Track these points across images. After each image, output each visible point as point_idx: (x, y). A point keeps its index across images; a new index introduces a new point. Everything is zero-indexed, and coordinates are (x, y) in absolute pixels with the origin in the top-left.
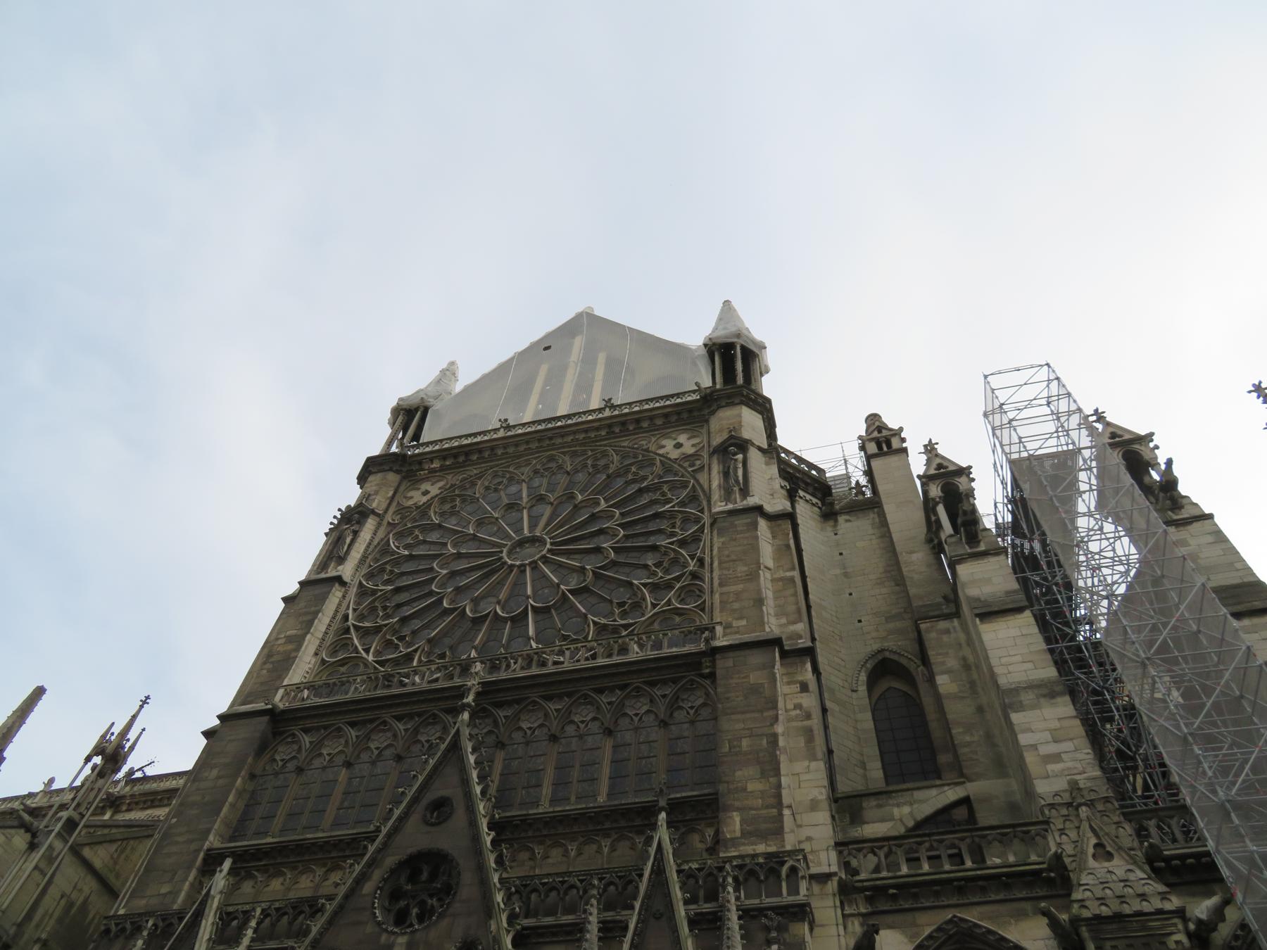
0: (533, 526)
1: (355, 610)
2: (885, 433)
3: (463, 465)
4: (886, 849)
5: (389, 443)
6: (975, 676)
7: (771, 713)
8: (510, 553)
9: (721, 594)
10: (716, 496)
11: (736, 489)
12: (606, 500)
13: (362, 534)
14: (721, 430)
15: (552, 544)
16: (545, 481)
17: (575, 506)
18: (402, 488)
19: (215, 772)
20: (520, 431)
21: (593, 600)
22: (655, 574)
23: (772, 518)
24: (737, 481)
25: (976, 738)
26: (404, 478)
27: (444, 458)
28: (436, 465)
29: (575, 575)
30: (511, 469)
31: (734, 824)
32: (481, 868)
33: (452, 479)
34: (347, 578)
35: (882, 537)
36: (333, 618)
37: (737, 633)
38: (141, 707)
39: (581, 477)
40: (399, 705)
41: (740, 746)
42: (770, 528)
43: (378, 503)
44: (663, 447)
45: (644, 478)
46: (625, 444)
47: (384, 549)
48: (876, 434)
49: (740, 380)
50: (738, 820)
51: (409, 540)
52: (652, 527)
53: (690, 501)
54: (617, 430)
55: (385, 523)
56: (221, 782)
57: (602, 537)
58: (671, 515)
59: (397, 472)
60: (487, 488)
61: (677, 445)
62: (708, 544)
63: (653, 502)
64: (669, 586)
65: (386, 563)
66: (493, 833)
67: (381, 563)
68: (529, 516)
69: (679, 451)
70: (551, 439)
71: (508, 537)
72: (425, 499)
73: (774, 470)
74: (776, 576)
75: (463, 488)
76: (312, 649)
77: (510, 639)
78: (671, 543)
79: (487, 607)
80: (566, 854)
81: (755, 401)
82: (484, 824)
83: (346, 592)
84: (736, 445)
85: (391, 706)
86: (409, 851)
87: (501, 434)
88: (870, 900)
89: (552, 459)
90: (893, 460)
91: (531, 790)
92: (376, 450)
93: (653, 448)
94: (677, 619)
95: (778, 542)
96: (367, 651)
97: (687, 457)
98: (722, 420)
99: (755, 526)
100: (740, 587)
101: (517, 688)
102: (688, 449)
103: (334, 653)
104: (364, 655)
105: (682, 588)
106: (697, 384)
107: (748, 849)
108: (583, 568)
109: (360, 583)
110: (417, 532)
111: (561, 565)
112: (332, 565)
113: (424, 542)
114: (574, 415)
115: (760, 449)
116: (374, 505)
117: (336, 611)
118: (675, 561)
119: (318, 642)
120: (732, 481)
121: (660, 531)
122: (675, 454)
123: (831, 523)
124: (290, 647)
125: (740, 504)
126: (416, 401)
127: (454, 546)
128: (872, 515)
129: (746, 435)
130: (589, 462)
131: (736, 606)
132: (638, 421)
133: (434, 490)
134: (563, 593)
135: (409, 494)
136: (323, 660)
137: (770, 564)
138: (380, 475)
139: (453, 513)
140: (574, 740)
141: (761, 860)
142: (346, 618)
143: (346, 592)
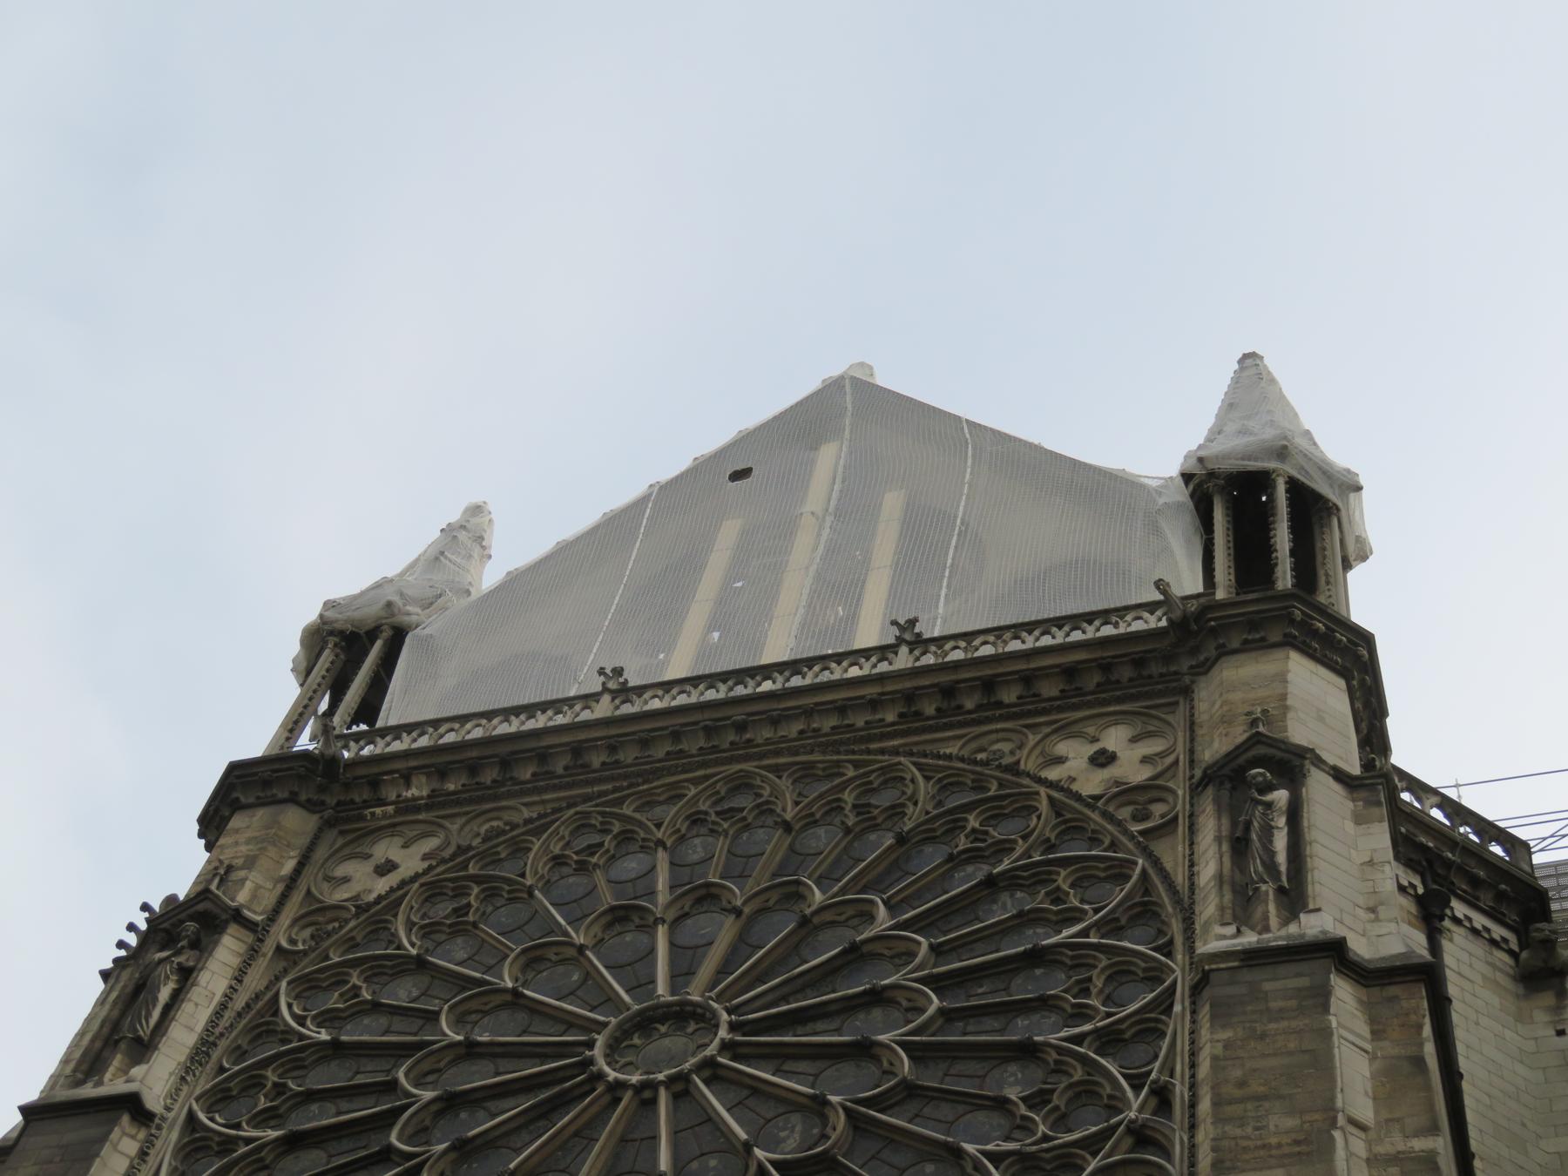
0: (680, 975)
5: (293, 726)
10: (1208, 907)
11: (1268, 888)
13: (204, 978)
14: (1226, 720)
15: (733, 1027)
16: (721, 845)
17: (804, 921)
18: (321, 853)
20: (656, 704)
22: (1026, 1126)
23: (1368, 976)
24: (1271, 867)
26: (328, 824)
27: (442, 773)
29: (796, 1119)
30: (627, 810)
33: (462, 831)
34: (154, 1101)
39: (823, 839)
42: (1367, 1007)
43: (251, 892)
44: (1060, 760)
45: (1004, 848)
47: (263, 1023)
49: (1285, 578)
51: (334, 1001)
52: (1023, 988)
53: (1134, 920)
54: (930, 709)
55: (268, 948)
57: (877, 1013)
58: (1076, 958)
59: (311, 806)
60: (558, 861)
61: (1097, 758)
62: (1183, 1044)
63: (1025, 919)
67: (251, 1058)
68: (672, 944)
70: (741, 727)
71: (610, 1001)
72: (382, 885)
73: (1380, 838)
74: (1380, 1149)
78: (1078, 1039)
81: (1327, 640)
84: (1266, 763)
87: (603, 709)
89: (742, 784)
92: (255, 743)
93: (1029, 765)
95: (1389, 1048)
97: (1126, 793)
98: (1233, 688)
99: (1321, 998)
102: (1132, 767)
106: (1160, 585)
108: (818, 1106)
109: (191, 1116)
110: (355, 979)
111: (757, 1089)
112: (117, 1061)
113: (376, 1007)
114: (810, 662)
115: (1339, 775)
116: (242, 897)
118: (1086, 1093)
120: (1256, 866)
121: (1044, 1003)
122: (1092, 783)
123: (1548, 998)
125: (1279, 934)
126: (372, 612)
127: (459, 1021)
129: (1299, 732)
130: (848, 797)
132: (989, 685)
133: (410, 861)
135: (340, 871)
137: (1365, 1111)
138: (261, 814)
139: (459, 927)
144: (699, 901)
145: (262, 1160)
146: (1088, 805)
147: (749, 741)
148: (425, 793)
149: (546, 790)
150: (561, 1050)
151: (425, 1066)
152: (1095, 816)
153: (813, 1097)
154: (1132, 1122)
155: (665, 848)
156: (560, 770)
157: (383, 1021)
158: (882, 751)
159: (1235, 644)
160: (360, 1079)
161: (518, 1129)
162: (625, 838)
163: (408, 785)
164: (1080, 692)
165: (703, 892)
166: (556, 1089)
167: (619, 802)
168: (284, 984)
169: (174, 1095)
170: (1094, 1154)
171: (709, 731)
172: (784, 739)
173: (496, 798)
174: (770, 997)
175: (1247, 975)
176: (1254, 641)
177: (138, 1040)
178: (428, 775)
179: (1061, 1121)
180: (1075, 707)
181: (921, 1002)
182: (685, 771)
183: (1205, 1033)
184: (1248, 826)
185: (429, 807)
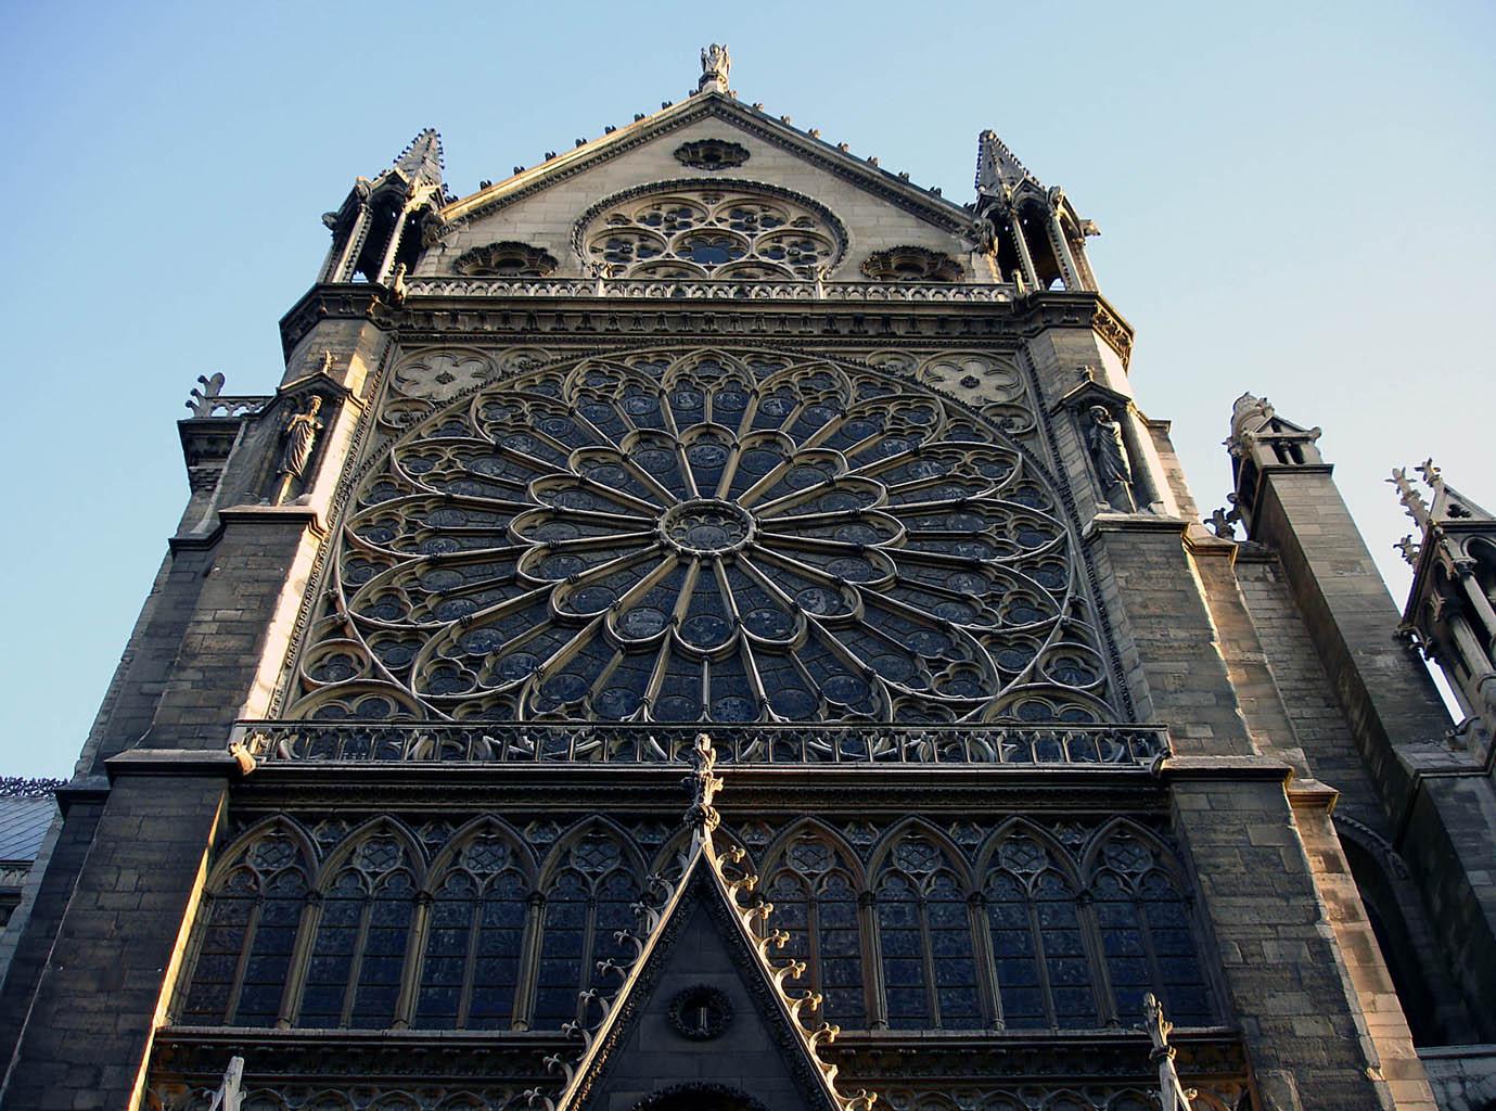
1: (349, 592)
2: (1286, 432)
5: (330, 270)
7: (1303, 901)
10: (1084, 490)
19: (129, 878)
24: (1123, 470)
27: (482, 318)
29: (818, 593)
40: (518, 795)
41: (1261, 954)
48: (1269, 432)
50: (1291, 1082)
56: (148, 899)
58: (993, 511)
62: (1084, 576)
65: (397, 505)
69: (973, 393)
70: (709, 320)
72: (446, 392)
78: (1011, 564)
85: (501, 795)
86: (660, 1085)
90: (1311, 485)
94: (1057, 709)
101: (775, 794)
104: (399, 684)
108: (838, 583)
122: (968, 397)
124: (232, 643)
131: (1184, 699)
134: (810, 623)
136: (301, 679)
138: (343, 324)
142: (331, 604)
145: (414, 573)
146: (972, 412)
147: (716, 331)
150: (628, 525)
154: (1063, 621)
155: (757, 397)
156: (572, 329)
158: (813, 353)
159: (1055, 322)
165: (705, 430)
166: (640, 551)
172: (740, 334)
174: (776, 509)
175: (1124, 537)
176: (1070, 322)
178: (470, 317)
180: (945, 345)
182: (668, 345)
183: (1104, 570)
184: (1099, 441)
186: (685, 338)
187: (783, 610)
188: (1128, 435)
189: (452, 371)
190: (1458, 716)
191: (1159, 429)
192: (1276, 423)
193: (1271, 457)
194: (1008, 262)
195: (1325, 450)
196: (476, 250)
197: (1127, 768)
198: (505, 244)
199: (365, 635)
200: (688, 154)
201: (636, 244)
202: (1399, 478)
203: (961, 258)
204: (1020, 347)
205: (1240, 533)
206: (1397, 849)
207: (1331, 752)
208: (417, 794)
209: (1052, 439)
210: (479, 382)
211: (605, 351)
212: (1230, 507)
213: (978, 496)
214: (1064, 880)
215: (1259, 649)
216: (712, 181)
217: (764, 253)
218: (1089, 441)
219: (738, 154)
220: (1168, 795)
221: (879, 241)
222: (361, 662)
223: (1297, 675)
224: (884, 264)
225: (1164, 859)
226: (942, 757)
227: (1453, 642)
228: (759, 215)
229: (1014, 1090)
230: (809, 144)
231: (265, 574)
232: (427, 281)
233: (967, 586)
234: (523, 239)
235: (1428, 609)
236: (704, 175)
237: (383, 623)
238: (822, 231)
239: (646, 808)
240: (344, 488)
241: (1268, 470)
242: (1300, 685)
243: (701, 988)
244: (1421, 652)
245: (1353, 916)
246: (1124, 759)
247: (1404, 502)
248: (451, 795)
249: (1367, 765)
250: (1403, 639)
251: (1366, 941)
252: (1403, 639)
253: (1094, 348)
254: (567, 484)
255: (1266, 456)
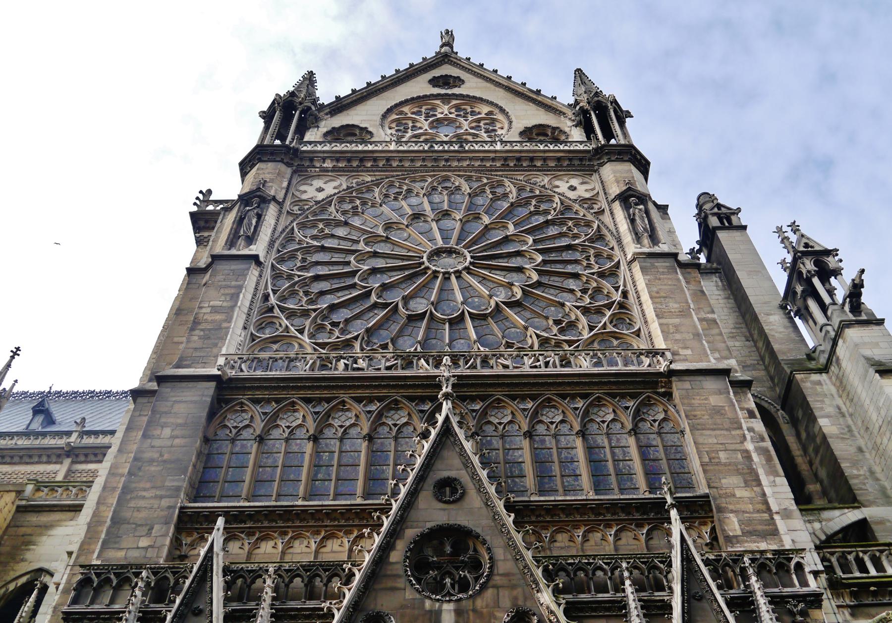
0: (445, 239)
1: (275, 292)
3: (357, 170)
4: (854, 554)
5: (263, 138)
6: (850, 422)
8: (429, 259)
9: (660, 325)
12: (516, 225)
15: (472, 257)
18: (294, 182)
21: (528, 314)
25: (862, 472)
26: (294, 172)
27: (338, 160)
28: (328, 164)
29: (501, 289)
30: (406, 182)
31: (733, 525)
32: (511, 545)
33: (343, 182)
34: (262, 259)
35: (728, 298)
36: (255, 295)
37: (686, 360)
38: (13, 357)
40: (359, 387)
46: (521, 178)
48: (716, 210)
50: (735, 520)
52: (566, 256)
53: (597, 239)
55: (284, 211)
59: (288, 165)
61: (570, 187)
62: (629, 279)
63: (562, 235)
64: (599, 311)
66: (513, 515)
70: (447, 160)
72: (320, 196)
75: (359, 191)
76: (241, 324)
77: (451, 341)
78: (593, 274)
79: (420, 306)
80: (571, 540)
82: (500, 505)
83: (261, 271)
85: (350, 388)
86: (429, 525)
88: (854, 595)
90: (736, 234)
91: (517, 480)
94: (615, 343)
96: (301, 332)
100: (677, 321)
102: (583, 191)
103: (260, 328)
104: (299, 336)
105: (613, 315)
107: (753, 546)
116: (272, 193)
117: (256, 289)
119: (244, 316)
121: (576, 262)
122: (572, 195)
128: (715, 279)
133: (330, 189)
134: (497, 303)
136: (252, 333)
139: (355, 212)
140: (547, 438)
141: (769, 556)
142: (266, 297)
143: (261, 271)
144: (444, 215)
148: (331, 166)
149: (377, 171)
150: (410, 258)
151: (359, 258)
152: (577, 205)
153: (508, 283)
156: (381, 165)
157: (336, 241)
159: (613, 159)
160: (333, 260)
161: (401, 283)
162: (409, 191)
163: (324, 162)
164: (561, 166)
167: (405, 179)
168: (295, 224)
169: (266, 257)
170: (609, 309)
171: (436, 160)
172: (462, 166)
173: (358, 171)
175: (648, 260)
177: (248, 237)
179: (592, 298)
180: (560, 171)
181: (535, 256)
184: (634, 214)
185: (332, 171)
186: (435, 168)
187: (484, 297)
188: (647, 212)
189: (323, 186)
190: (811, 345)
191: (663, 209)
192: (719, 206)
193: (716, 220)
194: (589, 131)
195: (743, 218)
196: (334, 128)
197: (651, 370)
198: (348, 125)
199: (282, 312)
200: (434, 82)
201: (410, 124)
202: (779, 230)
203: (567, 130)
204: (595, 171)
205: (703, 259)
206: (783, 409)
207: (749, 362)
208: (309, 388)
209: (612, 213)
210: (336, 191)
211: (398, 175)
212: (697, 247)
213: (577, 242)
214: (622, 424)
215: (713, 312)
216: (447, 94)
217: (472, 128)
218: (629, 215)
219: (458, 81)
220: (671, 382)
221: (527, 122)
222: (281, 325)
223: (732, 326)
224: (528, 133)
225: (669, 413)
226: (562, 366)
227: (807, 308)
228: (469, 110)
229: (600, 525)
230: (493, 77)
231: (234, 283)
232: (310, 143)
233: (572, 284)
234: (356, 123)
235: (795, 293)
236: (443, 91)
237: (292, 306)
238: (500, 117)
239: (419, 392)
240: (271, 243)
241: (716, 228)
242: (734, 331)
243: (449, 478)
244: (792, 314)
245: (762, 439)
246: (649, 365)
247: (782, 242)
248: (325, 388)
249: (766, 369)
250: (783, 307)
251: (768, 451)
252: (783, 307)
253: (630, 171)
254: (379, 239)
255: (714, 222)
